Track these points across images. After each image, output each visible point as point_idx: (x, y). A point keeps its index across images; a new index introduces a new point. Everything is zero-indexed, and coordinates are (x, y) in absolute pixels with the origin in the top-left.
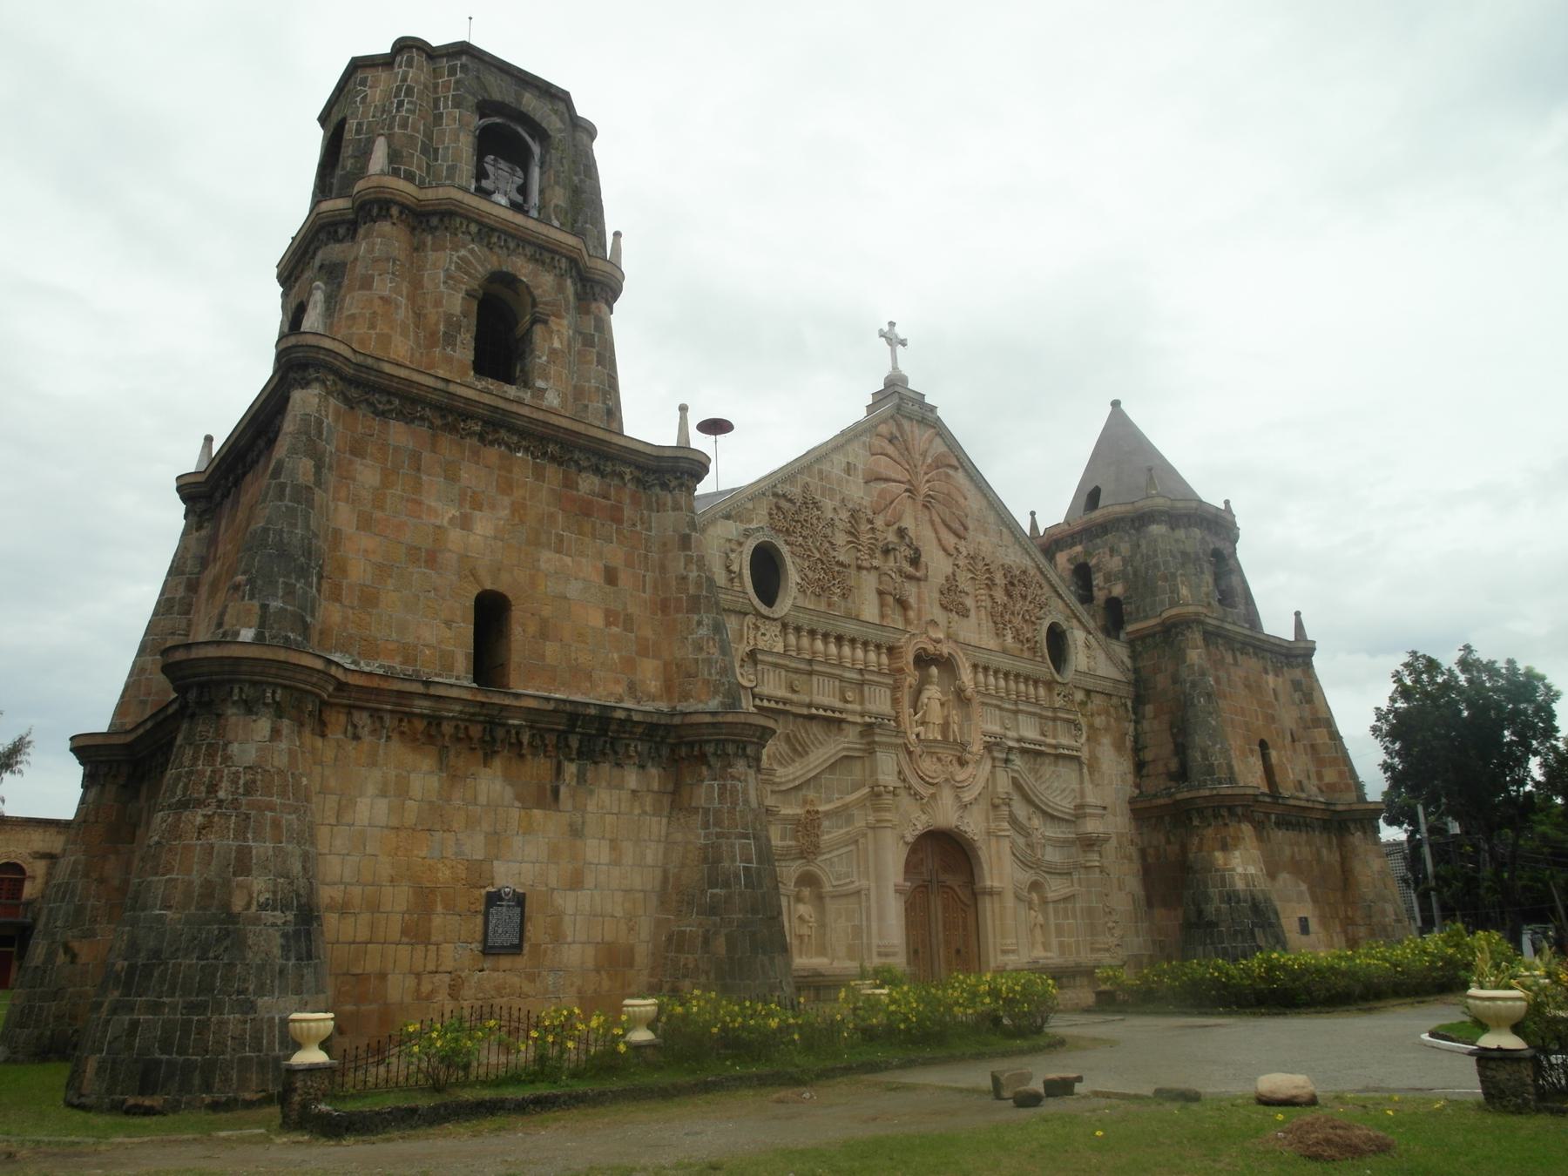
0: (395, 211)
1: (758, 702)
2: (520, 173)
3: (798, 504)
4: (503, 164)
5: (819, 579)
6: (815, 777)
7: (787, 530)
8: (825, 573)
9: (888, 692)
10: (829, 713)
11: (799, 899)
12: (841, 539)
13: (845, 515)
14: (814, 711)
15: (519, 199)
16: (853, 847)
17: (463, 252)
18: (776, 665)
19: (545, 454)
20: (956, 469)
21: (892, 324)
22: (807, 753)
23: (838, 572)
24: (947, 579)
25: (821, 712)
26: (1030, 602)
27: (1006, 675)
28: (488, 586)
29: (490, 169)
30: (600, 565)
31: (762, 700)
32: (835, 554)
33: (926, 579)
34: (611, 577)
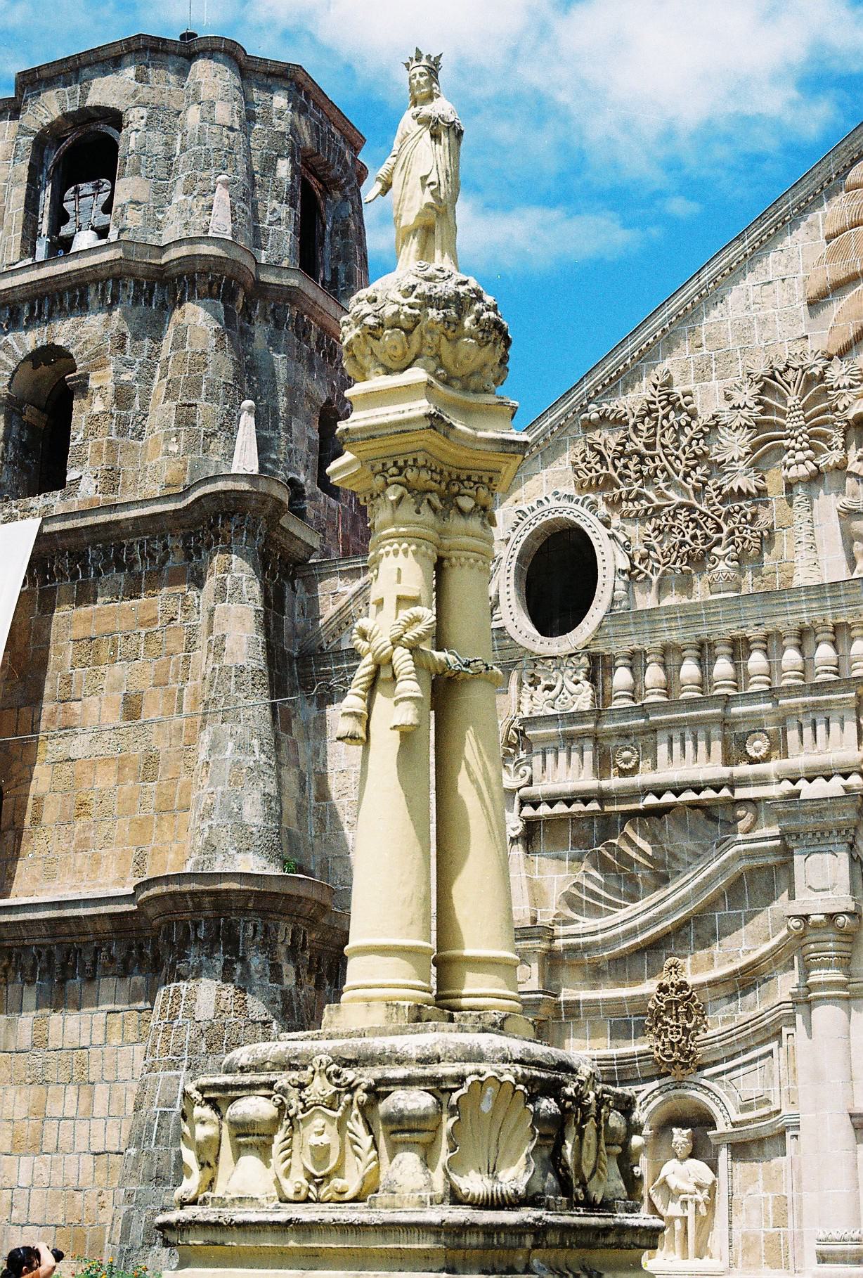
1: (528, 811)
3: (632, 422)
4: (86, 188)
5: (683, 544)
7: (608, 479)
8: (698, 526)
10: (689, 796)
12: (733, 445)
13: (747, 395)
14: (651, 800)
16: (773, 1045)
18: (569, 738)
19: (52, 574)
23: (729, 514)
25: (668, 798)
30: (119, 697)
31: (535, 806)
32: (724, 480)
34: (131, 708)
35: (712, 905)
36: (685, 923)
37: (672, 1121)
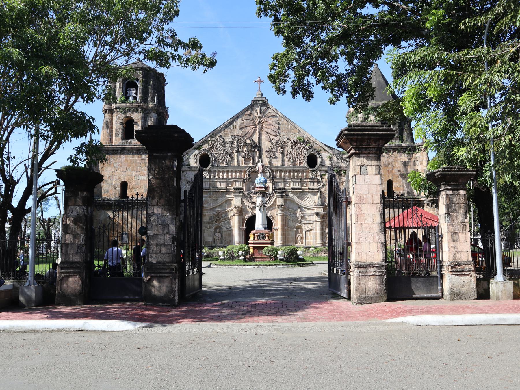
0: (107, 111)
2: (135, 90)
4: (132, 89)
6: (221, 205)
9: (242, 183)
11: (216, 232)
14: (217, 190)
15: (135, 96)
17: (119, 115)
20: (276, 116)
21: (259, 78)
22: (217, 200)
24: (269, 149)
26: (302, 149)
27: (290, 172)
28: (123, 180)
29: (128, 92)
33: (260, 150)
35: (222, 203)
36: (219, 205)
37: (216, 228)
